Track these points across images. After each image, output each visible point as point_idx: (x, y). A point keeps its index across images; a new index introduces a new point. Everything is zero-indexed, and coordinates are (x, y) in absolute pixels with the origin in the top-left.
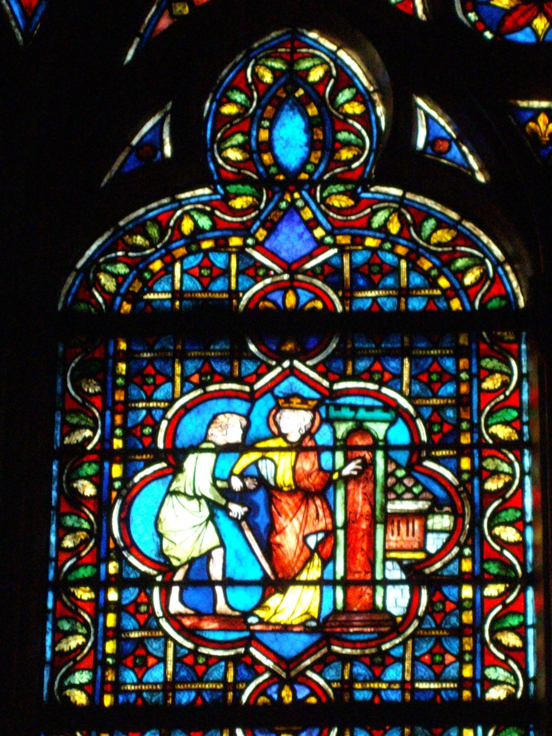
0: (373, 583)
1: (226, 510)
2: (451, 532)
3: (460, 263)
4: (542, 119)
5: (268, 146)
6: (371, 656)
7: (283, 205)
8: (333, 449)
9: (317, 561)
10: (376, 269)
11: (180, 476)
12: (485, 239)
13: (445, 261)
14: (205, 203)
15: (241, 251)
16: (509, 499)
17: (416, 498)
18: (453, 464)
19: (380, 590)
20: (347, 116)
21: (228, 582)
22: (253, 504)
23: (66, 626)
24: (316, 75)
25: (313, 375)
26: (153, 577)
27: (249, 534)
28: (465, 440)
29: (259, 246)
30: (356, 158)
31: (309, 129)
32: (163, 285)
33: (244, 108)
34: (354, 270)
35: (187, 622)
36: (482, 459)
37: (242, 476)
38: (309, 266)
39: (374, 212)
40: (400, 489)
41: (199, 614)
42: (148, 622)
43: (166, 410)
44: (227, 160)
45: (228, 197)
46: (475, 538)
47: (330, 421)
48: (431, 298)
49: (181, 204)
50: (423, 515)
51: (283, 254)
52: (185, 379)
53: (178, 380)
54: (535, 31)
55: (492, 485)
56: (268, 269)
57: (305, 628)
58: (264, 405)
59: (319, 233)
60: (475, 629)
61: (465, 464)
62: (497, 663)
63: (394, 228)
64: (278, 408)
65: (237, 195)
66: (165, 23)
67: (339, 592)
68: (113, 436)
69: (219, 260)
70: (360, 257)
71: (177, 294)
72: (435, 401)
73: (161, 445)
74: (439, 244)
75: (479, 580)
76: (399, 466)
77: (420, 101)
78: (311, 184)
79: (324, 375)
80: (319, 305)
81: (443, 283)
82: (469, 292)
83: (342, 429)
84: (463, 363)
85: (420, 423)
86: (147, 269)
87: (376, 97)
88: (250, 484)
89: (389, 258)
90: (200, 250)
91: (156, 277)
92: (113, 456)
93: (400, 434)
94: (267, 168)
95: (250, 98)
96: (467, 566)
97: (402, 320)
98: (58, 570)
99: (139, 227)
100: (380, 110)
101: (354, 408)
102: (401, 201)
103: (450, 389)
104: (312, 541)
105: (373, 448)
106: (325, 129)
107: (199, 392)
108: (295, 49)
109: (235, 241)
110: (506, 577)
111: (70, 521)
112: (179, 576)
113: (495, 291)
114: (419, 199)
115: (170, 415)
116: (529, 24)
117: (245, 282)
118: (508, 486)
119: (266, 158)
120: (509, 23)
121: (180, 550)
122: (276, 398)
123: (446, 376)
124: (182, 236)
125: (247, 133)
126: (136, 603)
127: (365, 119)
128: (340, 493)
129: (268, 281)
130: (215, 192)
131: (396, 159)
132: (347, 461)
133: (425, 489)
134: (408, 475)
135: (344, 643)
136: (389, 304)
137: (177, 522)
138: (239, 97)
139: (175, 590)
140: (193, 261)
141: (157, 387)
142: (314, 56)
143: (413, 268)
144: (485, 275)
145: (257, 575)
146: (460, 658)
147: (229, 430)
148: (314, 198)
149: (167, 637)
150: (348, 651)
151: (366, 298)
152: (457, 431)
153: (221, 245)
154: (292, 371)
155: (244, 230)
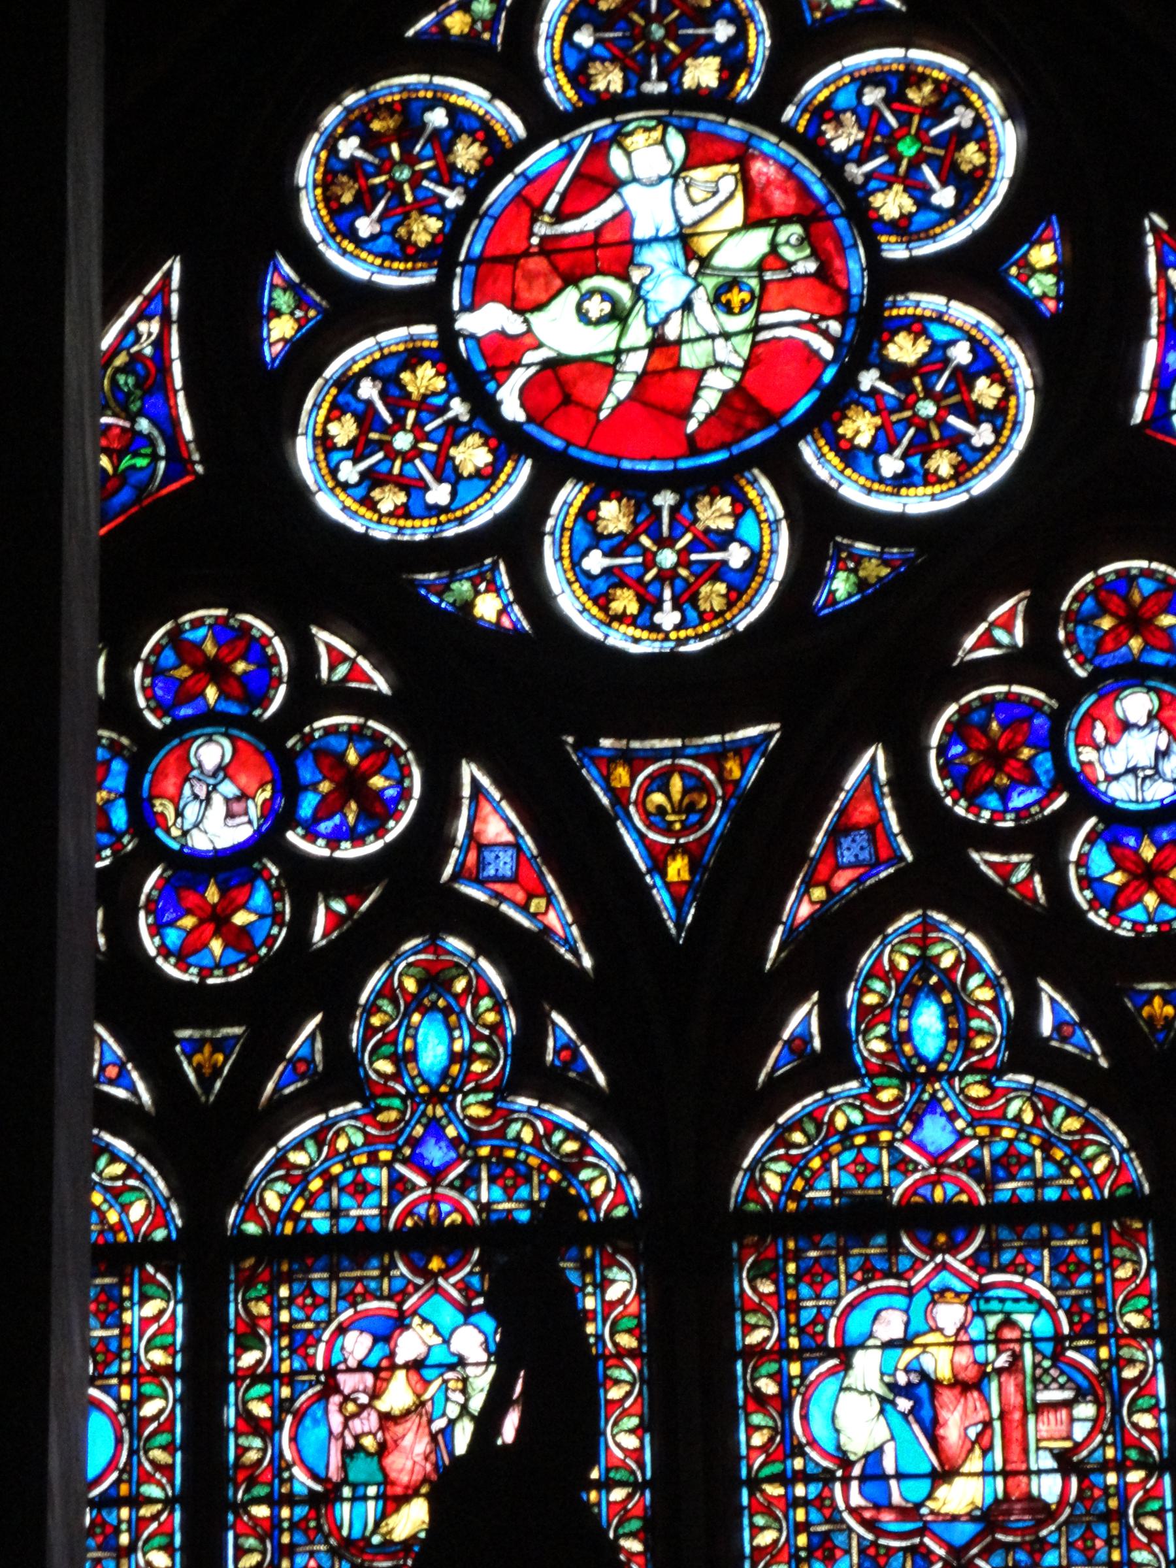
0: (1028, 1473)
1: (893, 1403)
2: (1096, 1421)
3: (1090, 1151)
4: (1157, 1001)
5: (907, 1036)
6: (1031, 1543)
7: (926, 1097)
8: (986, 1342)
9: (977, 1451)
10: (1014, 1160)
11: (852, 1373)
12: (1111, 1126)
13: (1076, 1148)
14: (855, 1097)
15: (890, 1145)
16: (1144, 1385)
17: (1062, 1387)
18: (1092, 1352)
19: (1034, 1478)
20: (978, 1002)
21: (900, 1476)
22: (918, 1397)
23: (760, 1520)
24: (947, 961)
25: (964, 1269)
26: (832, 1472)
27: (916, 1427)
28: (1103, 1330)
29: (906, 1139)
30: (989, 1046)
31: (945, 1017)
32: (822, 1183)
33: (884, 997)
34: (995, 1161)
35: (867, 1515)
36: (1119, 1348)
37: (907, 1370)
38: (953, 1158)
39: (1009, 1101)
40: (1047, 1380)
41: (877, 1507)
42: (833, 1517)
43: (834, 1308)
44: (872, 1052)
45: (875, 1090)
46: (1116, 1426)
47: (980, 1314)
48: (1064, 1188)
49: (832, 1098)
50: (1068, 1404)
51: (931, 1149)
52: (849, 1277)
53: (843, 1277)
54: (1146, 908)
55: (1129, 1373)
56: (916, 1164)
57: (971, 1518)
58: (923, 1297)
59: (960, 1124)
60: (1121, 1514)
61: (1104, 1353)
62: (1142, 1547)
63: (1028, 1117)
64: (934, 1302)
65: (883, 1088)
66: (805, 910)
67: (1000, 1481)
68: (789, 1335)
69: (871, 1155)
70: (999, 1148)
71: (836, 1192)
72: (1073, 1292)
73: (831, 1343)
74: (1069, 1133)
75: (1121, 1467)
76: (1045, 1357)
77: (1043, 984)
78: (950, 1075)
79: (973, 1268)
80: (964, 1198)
81: (1075, 1172)
82: (1098, 1180)
83: (993, 1321)
84: (1097, 1253)
85: (1061, 1314)
86: (806, 1167)
87: (1004, 981)
88: (915, 1378)
89: (1024, 1148)
90: (853, 1146)
91: (815, 1174)
92: (792, 1355)
93: (1043, 1326)
94: (909, 1059)
95: (889, 987)
96: (1110, 1453)
97: (1038, 1211)
98: (750, 1468)
99: (796, 1124)
100: (1008, 995)
101: (1002, 1300)
102: (1032, 1088)
103: (1084, 1279)
104: (972, 1433)
105: (1021, 1341)
106: (959, 1013)
107: (863, 1289)
108: (924, 935)
109: (885, 1136)
110: (1145, 1463)
111: (757, 1419)
112: (857, 1471)
113: (1122, 1180)
114: (1049, 1086)
115: (838, 1312)
116: (1140, 900)
117: (896, 1177)
118: (1143, 1373)
119: (907, 1048)
120: (1121, 901)
121: (856, 1445)
122: (932, 1293)
123: (1082, 1267)
124: (837, 1132)
125: (888, 1024)
126: (820, 1497)
127: (994, 1004)
128: (994, 1385)
129: (917, 1176)
130: (863, 1085)
131: (1025, 1048)
132: (999, 1352)
133: (1070, 1379)
134: (1054, 1366)
135: (1007, 1531)
136: (1027, 1195)
137: (851, 1415)
138: (878, 986)
139: (854, 1485)
140: (848, 1157)
141: (823, 1285)
142: (943, 940)
143: (1048, 1158)
144: (1112, 1161)
145: (926, 1469)
146: (1108, 1542)
147: (892, 1326)
148: (952, 1087)
149: (850, 1530)
150: (1010, 1539)
151: (1005, 1190)
152: (1095, 1321)
153: (873, 1140)
154: (944, 1266)
155: (891, 1124)
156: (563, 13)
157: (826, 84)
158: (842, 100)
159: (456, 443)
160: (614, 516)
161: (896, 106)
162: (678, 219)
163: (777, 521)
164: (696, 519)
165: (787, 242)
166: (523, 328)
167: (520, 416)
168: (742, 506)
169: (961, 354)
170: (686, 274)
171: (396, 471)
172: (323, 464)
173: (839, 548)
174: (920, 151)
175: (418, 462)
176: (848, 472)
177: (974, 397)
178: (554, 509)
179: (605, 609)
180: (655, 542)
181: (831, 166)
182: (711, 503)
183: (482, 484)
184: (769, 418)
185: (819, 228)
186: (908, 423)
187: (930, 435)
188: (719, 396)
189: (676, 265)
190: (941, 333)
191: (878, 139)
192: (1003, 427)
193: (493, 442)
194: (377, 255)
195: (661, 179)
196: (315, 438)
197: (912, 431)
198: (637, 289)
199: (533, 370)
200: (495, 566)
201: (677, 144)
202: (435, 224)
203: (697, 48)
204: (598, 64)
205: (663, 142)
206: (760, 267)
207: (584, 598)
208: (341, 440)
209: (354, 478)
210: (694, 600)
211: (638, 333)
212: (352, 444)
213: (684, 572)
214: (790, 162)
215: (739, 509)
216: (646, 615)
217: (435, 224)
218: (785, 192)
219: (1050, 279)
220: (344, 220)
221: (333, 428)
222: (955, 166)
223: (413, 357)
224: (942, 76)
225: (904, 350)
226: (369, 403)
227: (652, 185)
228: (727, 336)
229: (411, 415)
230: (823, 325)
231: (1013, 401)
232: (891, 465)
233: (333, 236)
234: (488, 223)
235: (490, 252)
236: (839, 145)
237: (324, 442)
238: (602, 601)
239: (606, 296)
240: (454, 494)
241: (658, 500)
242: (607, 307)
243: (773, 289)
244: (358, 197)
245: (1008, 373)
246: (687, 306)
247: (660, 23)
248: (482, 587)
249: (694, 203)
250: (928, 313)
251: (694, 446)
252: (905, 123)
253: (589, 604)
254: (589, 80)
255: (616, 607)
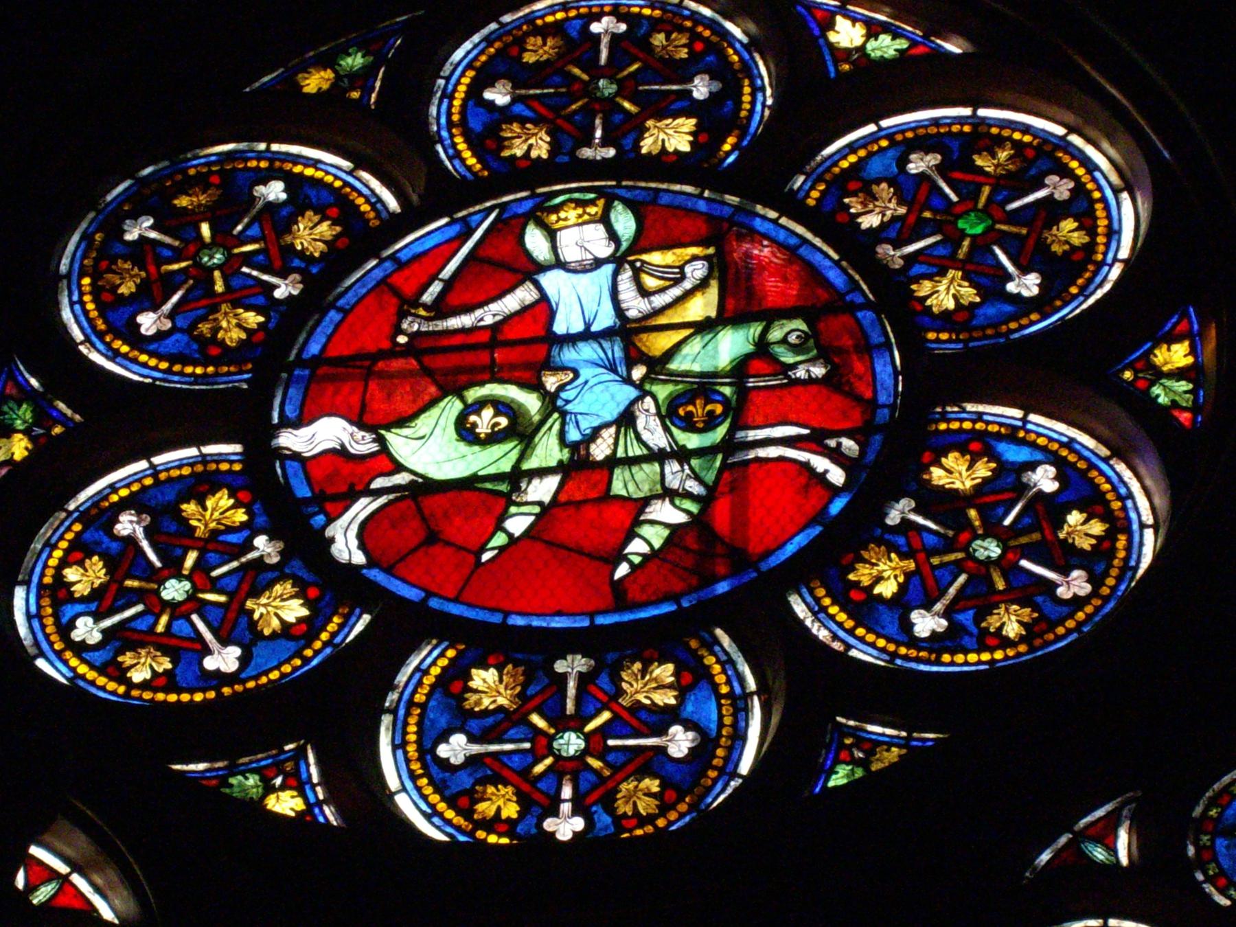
156: (470, 66)
157: (852, 148)
158: (876, 167)
159: (256, 593)
160: (489, 686)
161: (957, 175)
162: (619, 311)
163: (747, 696)
164: (621, 692)
165: (784, 341)
166: (374, 447)
167: (359, 558)
168: (692, 677)
169: (1045, 479)
170: (628, 381)
171: (160, 628)
172: (49, 621)
173: (843, 731)
174: (989, 230)
175: (195, 617)
176: (860, 631)
177: (1062, 535)
178: (402, 678)
179: (467, 813)
180: (551, 722)
181: (857, 246)
182: (644, 672)
183: (292, 646)
184: (740, 560)
185: (834, 325)
186: (958, 567)
187: (992, 584)
188: (666, 533)
189: (613, 369)
190: (1014, 454)
191: (927, 214)
192: (1106, 574)
193: (313, 592)
194: (161, 358)
195: (598, 263)
196: (41, 586)
197: (962, 579)
198: (551, 402)
199: (382, 500)
200: (300, 754)
201: (625, 223)
202: (253, 319)
203: (666, 108)
204: (516, 127)
205: (605, 220)
206: (740, 369)
207: (435, 798)
208: (81, 589)
209: (95, 638)
210: (609, 802)
211: (548, 451)
212: (97, 594)
213: (595, 763)
214: (793, 241)
215: (687, 678)
216: (531, 820)
217: (253, 319)
218: (785, 279)
219: (1183, 386)
220: (119, 316)
221: (71, 574)
222: (1043, 247)
223: (202, 483)
224: (1027, 139)
225: (956, 473)
226: (131, 540)
227: (585, 271)
228: (682, 455)
229: (191, 558)
230: (832, 443)
231: (1122, 542)
232: (925, 623)
233: (101, 335)
234: (334, 316)
235: (332, 353)
236: (870, 221)
237: (58, 592)
238: (463, 802)
239: (501, 406)
240: (244, 660)
241: (560, 666)
242: (504, 422)
243: (757, 399)
244: (143, 288)
245: (1116, 505)
246: (626, 420)
247: (612, 79)
248: (278, 781)
249: (644, 293)
250: (993, 428)
251: (620, 596)
252: (969, 194)
253: (442, 806)
254: (502, 143)
255: (485, 809)
